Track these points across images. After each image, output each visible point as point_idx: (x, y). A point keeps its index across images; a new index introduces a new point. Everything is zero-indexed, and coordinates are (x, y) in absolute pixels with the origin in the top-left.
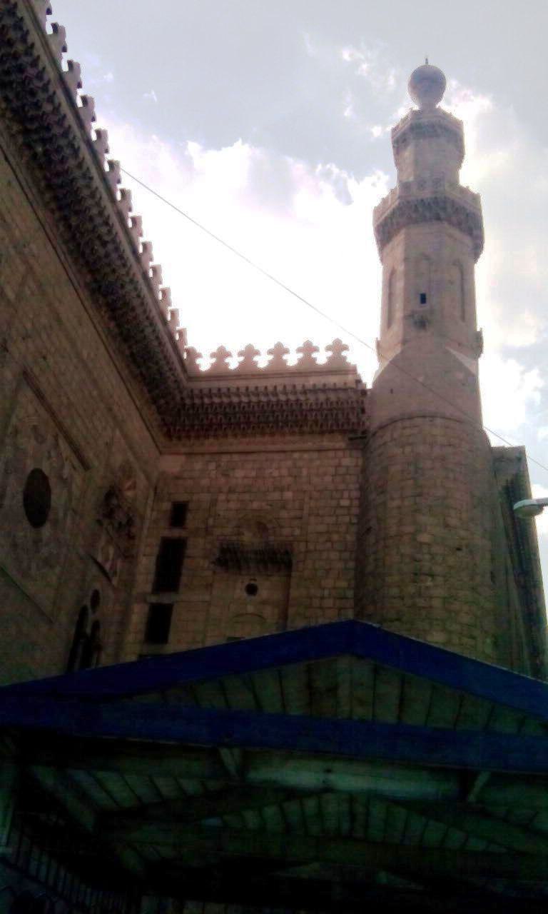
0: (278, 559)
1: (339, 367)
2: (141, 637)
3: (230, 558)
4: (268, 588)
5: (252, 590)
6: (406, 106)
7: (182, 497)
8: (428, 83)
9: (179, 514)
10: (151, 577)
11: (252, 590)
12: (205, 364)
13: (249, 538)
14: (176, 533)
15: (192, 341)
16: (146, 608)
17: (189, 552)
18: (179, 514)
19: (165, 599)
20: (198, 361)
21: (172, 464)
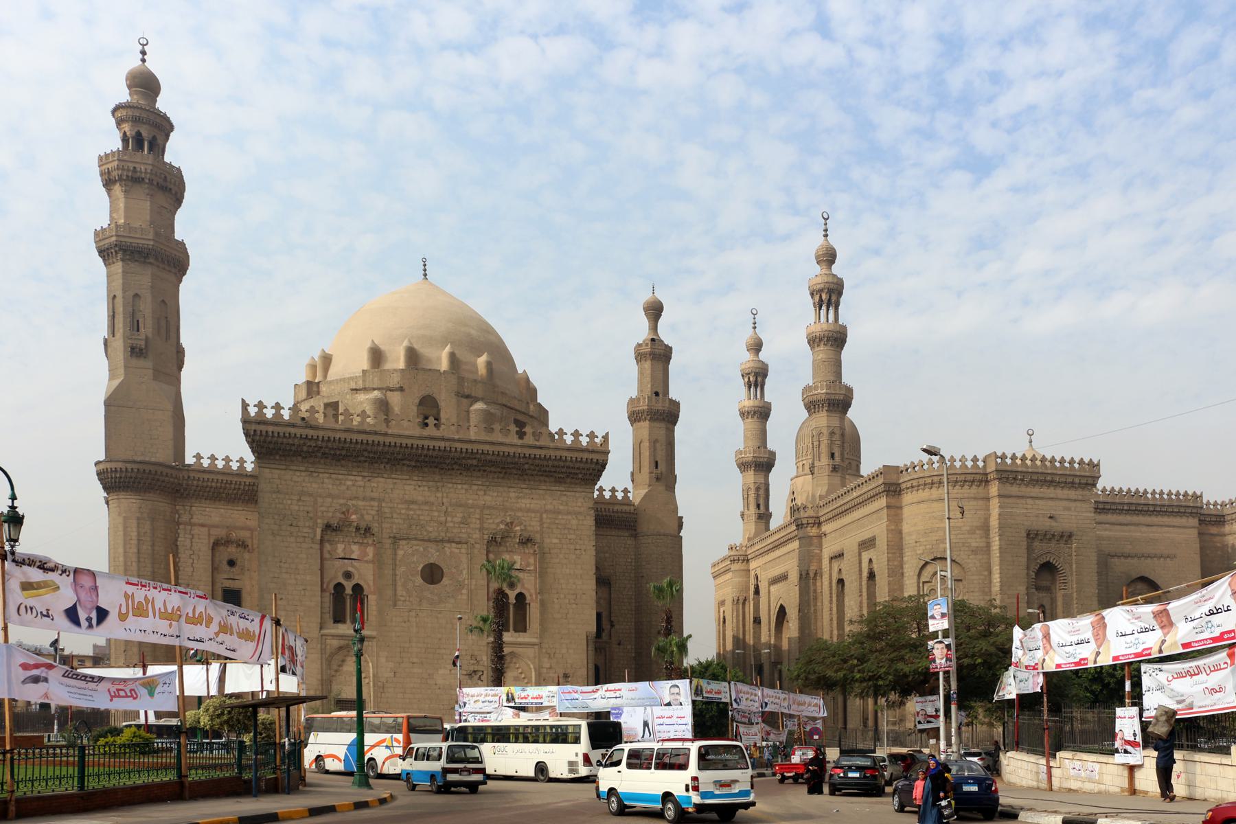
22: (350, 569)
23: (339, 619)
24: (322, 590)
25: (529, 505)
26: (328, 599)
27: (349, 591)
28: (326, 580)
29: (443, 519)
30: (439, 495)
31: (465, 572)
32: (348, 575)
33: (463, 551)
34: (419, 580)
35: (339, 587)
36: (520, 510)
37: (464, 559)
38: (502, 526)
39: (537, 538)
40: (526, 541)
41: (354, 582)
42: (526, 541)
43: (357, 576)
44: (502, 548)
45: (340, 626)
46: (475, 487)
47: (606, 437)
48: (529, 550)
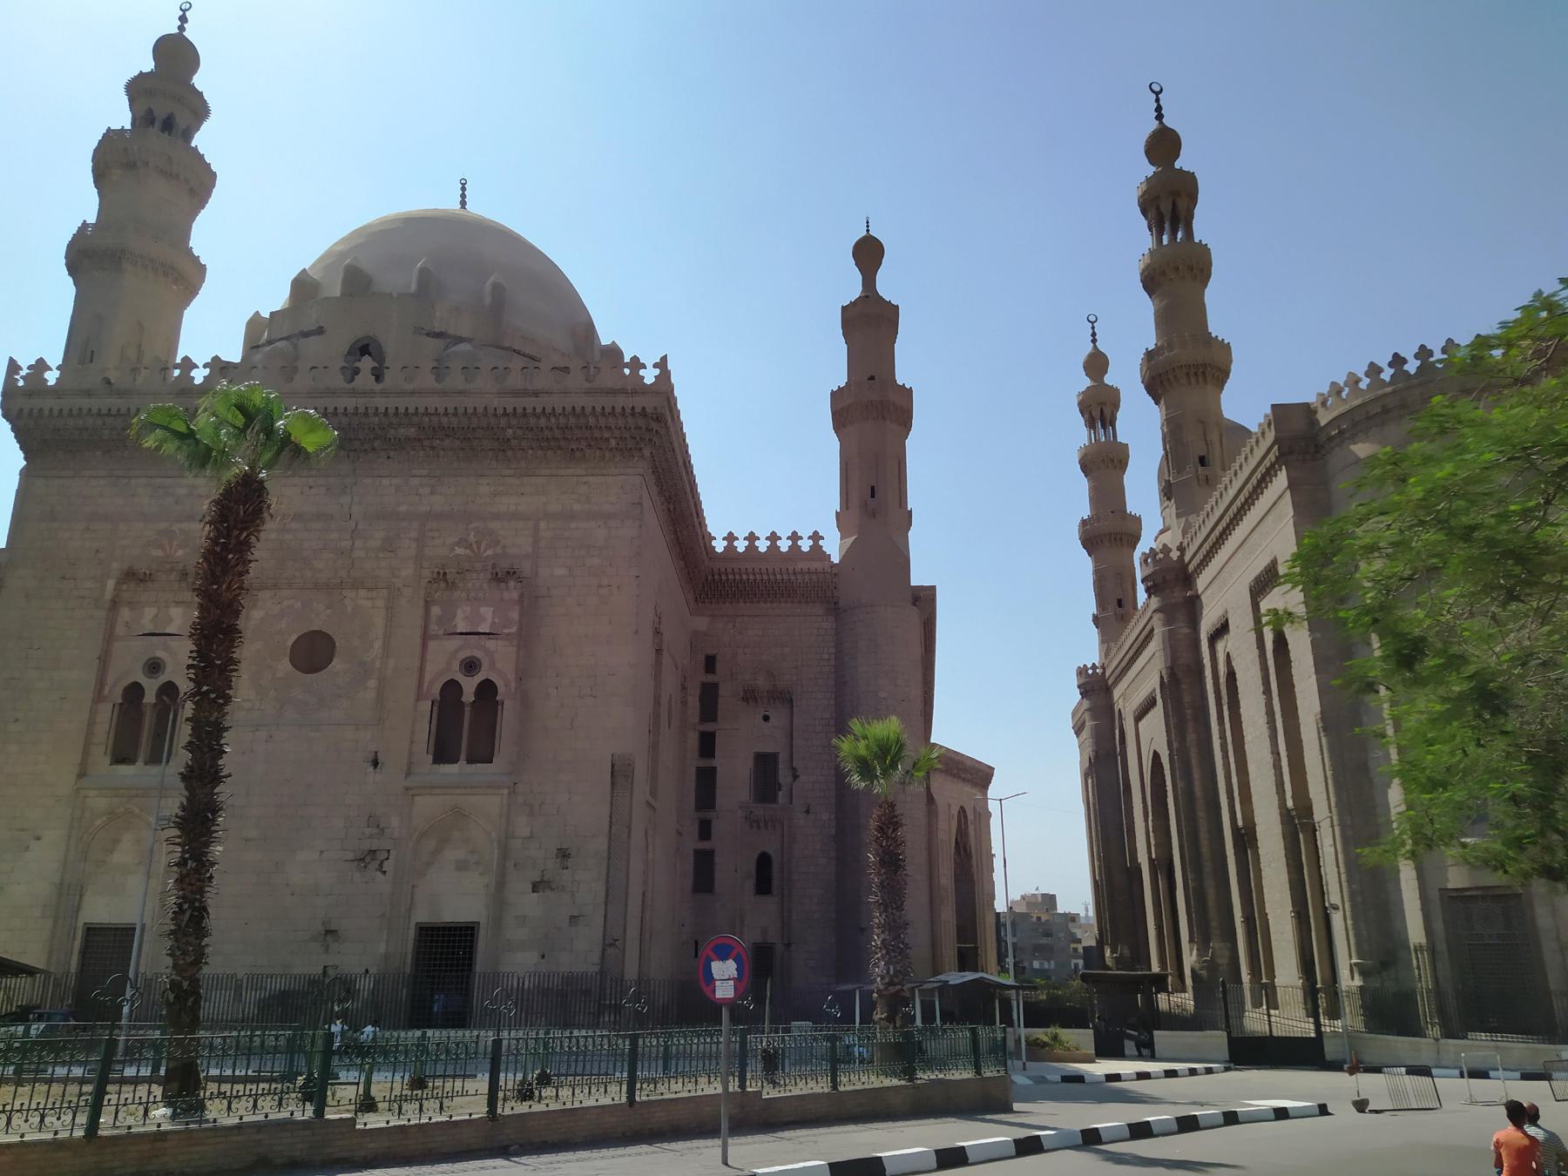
0: (784, 698)
1: (817, 551)
2: (696, 754)
3: (750, 696)
4: (778, 717)
5: (766, 718)
6: (853, 289)
7: (711, 652)
8: (868, 253)
9: (710, 664)
10: (698, 711)
11: (766, 718)
12: (719, 546)
13: (762, 683)
14: (710, 678)
15: (712, 527)
16: (696, 736)
17: (721, 692)
18: (710, 664)
19: (708, 727)
20: (714, 543)
21: (701, 623)
22: (160, 654)
23: (122, 756)
24: (99, 697)
25: (521, 506)
26: (106, 716)
27: (150, 697)
28: (110, 680)
29: (347, 544)
30: (346, 499)
31: (378, 644)
32: (154, 667)
33: (380, 603)
34: (285, 666)
35: (135, 691)
36: (497, 517)
37: (379, 620)
38: (459, 551)
39: (526, 568)
40: (503, 576)
41: (163, 678)
42: (503, 576)
43: (169, 669)
44: (457, 594)
45: (123, 769)
46: (415, 481)
47: (662, 364)
48: (512, 592)
